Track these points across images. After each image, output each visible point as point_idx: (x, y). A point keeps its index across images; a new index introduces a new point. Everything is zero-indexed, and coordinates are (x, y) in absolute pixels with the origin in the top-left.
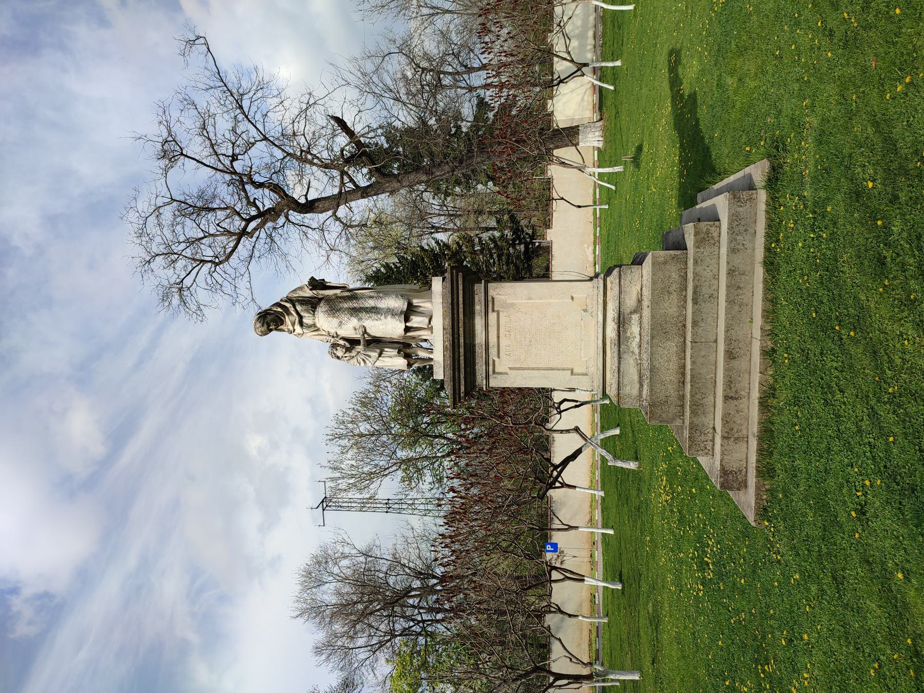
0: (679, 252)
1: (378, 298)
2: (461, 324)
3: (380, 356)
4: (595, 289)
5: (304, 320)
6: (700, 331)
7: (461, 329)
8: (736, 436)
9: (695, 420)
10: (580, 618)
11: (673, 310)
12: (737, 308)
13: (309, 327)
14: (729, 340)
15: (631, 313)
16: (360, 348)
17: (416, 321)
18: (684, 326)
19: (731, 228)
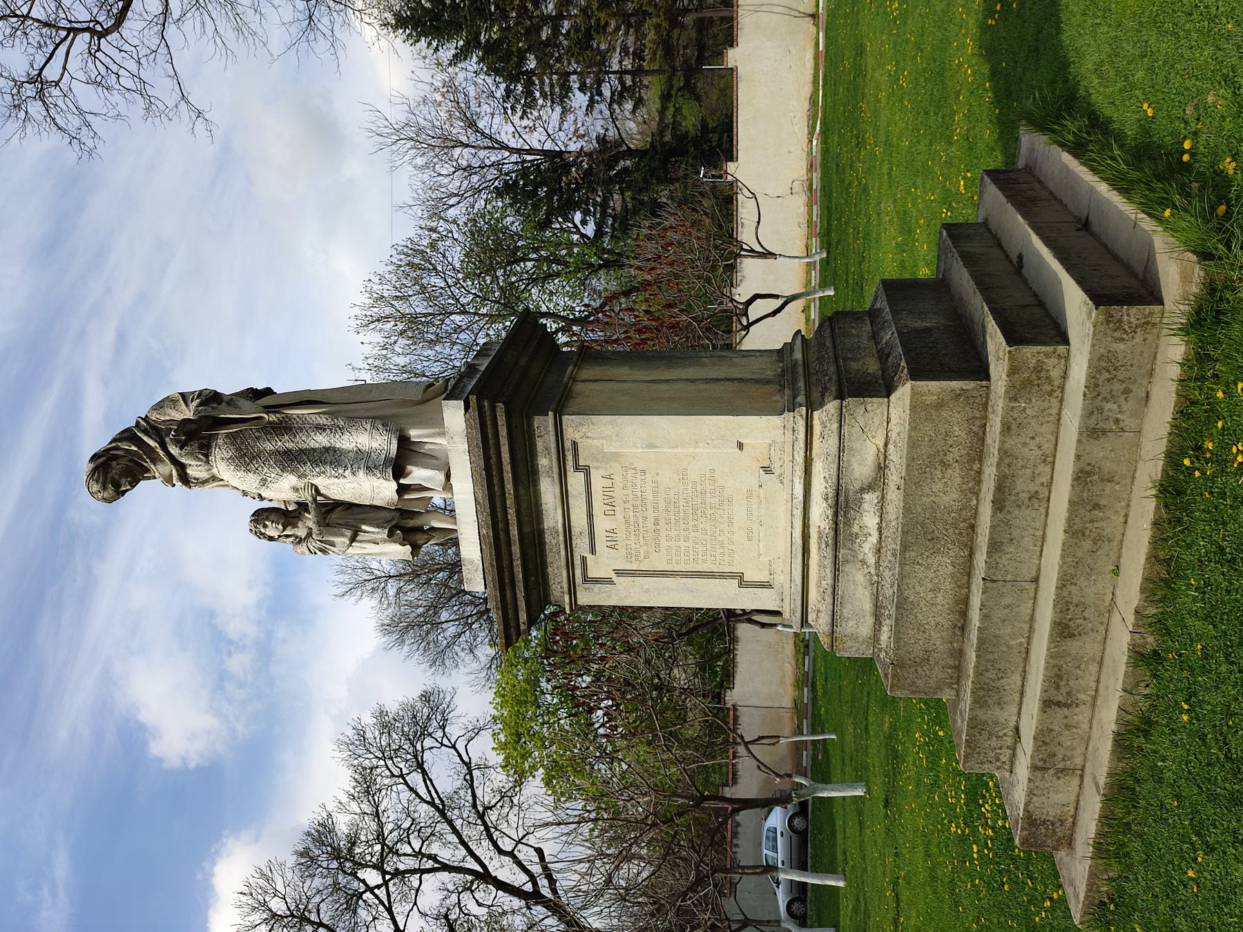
0: (970, 385)
1: (335, 429)
2: (510, 502)
6: (1004, 560)
7: (511, 512)
10: (780, 628)
18: (973, 527)
19: (1093, 385)
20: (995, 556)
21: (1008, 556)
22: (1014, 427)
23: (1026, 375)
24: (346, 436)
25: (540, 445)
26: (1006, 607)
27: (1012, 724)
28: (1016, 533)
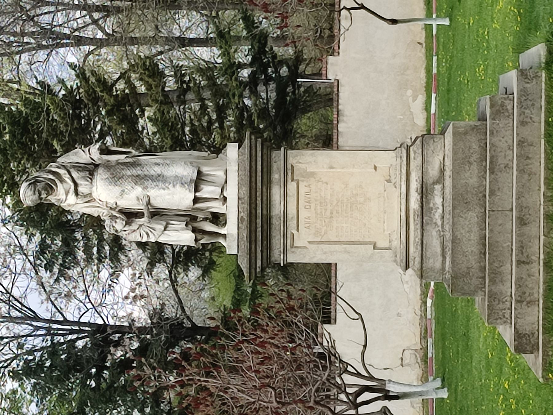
3: (165, 230)
4: (399, 159)
5: (80, 189)
6: (496, 199)
8: (528, 299)
9: (493, 288)
11: (473, 181)
12: (526, 176)
13: (85, 196)
14: (520, 208)
15: (434, 183)
16: (144, 220)
17: (207, 191)
20: (492, 197)
21: (498, 197)
22: (495, 132)
23: (498, 108)
24: (171, 168)
25: (275, 166)
26: (500, 225)
27: (509, 294)
28: (500, 185)
